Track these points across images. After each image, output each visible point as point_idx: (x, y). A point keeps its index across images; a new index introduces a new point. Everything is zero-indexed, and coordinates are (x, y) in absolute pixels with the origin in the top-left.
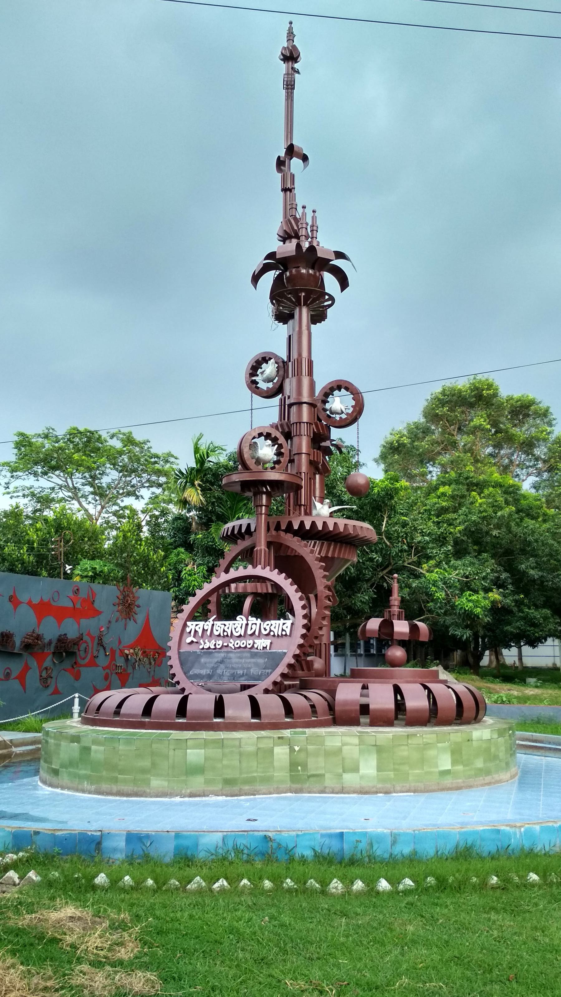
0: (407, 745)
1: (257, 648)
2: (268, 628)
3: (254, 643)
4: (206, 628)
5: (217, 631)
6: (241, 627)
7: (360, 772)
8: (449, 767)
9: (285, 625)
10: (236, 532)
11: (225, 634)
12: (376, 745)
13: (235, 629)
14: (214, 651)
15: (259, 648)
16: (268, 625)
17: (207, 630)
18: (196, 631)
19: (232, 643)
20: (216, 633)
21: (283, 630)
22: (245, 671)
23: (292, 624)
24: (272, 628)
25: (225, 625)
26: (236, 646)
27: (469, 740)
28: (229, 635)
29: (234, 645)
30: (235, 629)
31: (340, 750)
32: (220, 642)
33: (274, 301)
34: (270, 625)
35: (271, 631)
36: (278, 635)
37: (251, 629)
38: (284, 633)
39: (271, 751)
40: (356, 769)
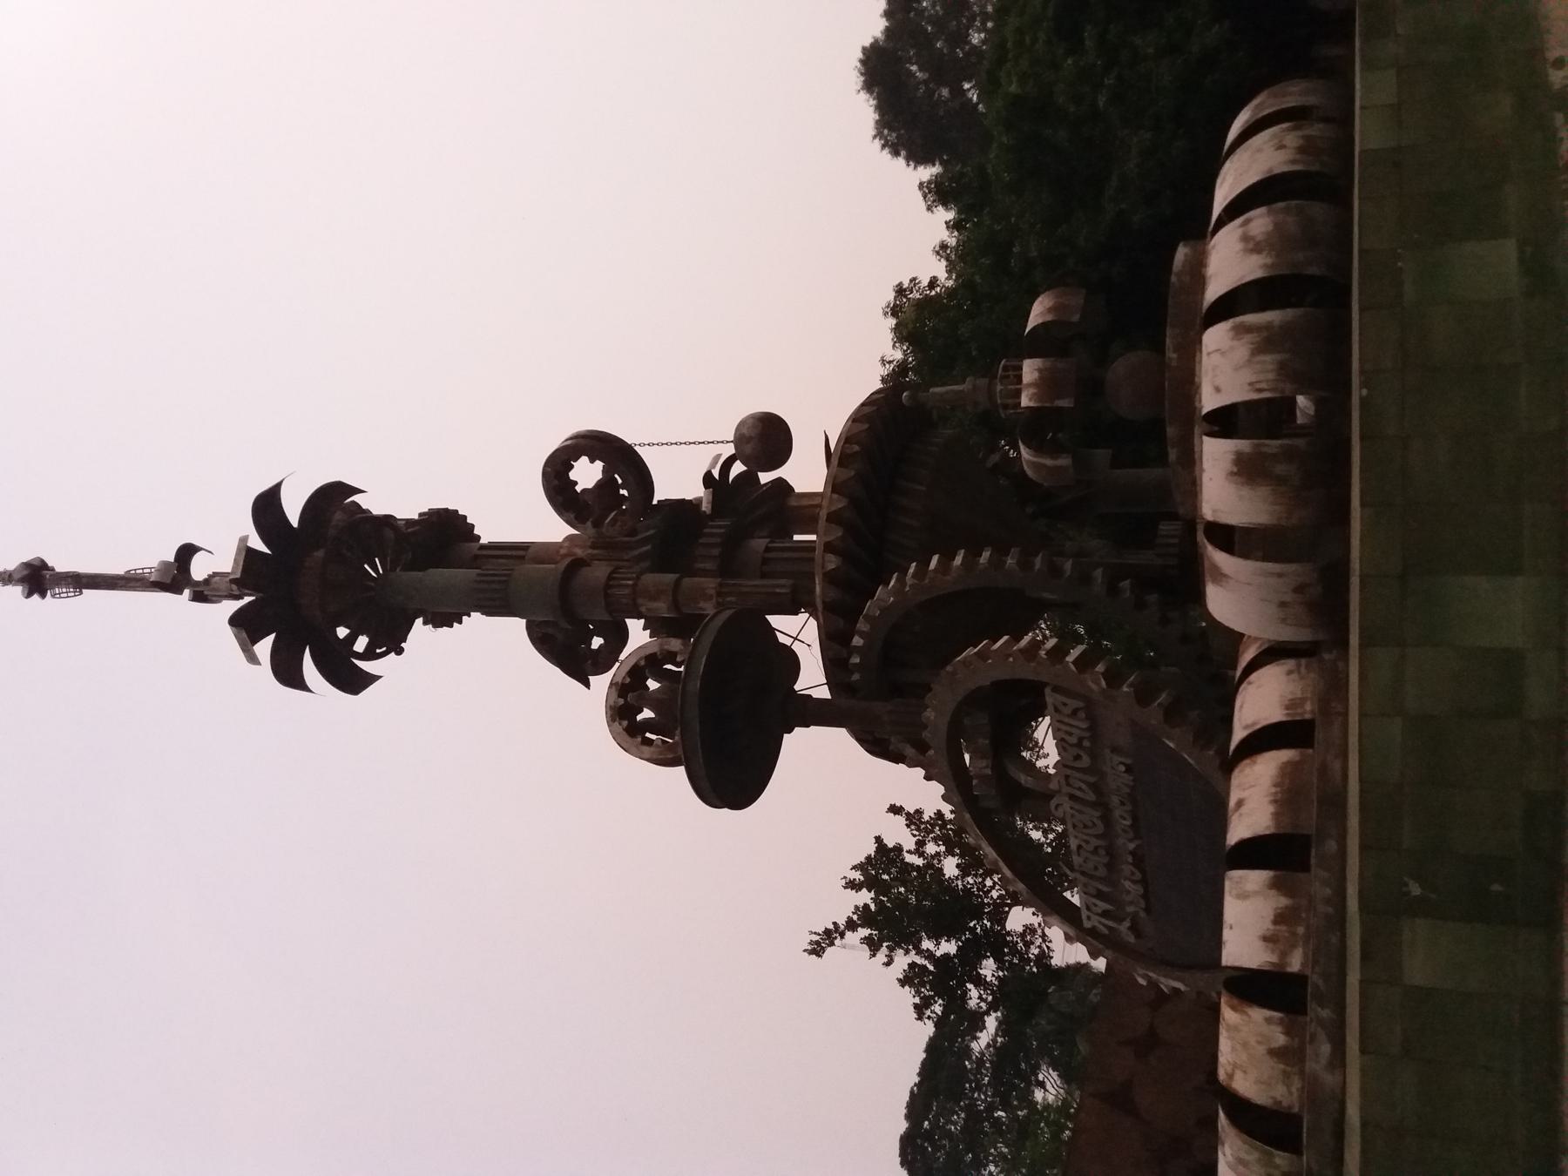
4: (1094, 892)
5: (1096, 868)
13: (1085, 826)
15: (1131, 784)
17: (1099, 891)
18: (1105, 914)
20: (1102, 872)
23: (1056, 689)
24: (1074, 740)
25: (1079, 847)
26: (1131, 835)
30: (1085, 826)
33: (378, 651)
35: (1079, 745)
36: (1088, 729)
37: (1080, 789)
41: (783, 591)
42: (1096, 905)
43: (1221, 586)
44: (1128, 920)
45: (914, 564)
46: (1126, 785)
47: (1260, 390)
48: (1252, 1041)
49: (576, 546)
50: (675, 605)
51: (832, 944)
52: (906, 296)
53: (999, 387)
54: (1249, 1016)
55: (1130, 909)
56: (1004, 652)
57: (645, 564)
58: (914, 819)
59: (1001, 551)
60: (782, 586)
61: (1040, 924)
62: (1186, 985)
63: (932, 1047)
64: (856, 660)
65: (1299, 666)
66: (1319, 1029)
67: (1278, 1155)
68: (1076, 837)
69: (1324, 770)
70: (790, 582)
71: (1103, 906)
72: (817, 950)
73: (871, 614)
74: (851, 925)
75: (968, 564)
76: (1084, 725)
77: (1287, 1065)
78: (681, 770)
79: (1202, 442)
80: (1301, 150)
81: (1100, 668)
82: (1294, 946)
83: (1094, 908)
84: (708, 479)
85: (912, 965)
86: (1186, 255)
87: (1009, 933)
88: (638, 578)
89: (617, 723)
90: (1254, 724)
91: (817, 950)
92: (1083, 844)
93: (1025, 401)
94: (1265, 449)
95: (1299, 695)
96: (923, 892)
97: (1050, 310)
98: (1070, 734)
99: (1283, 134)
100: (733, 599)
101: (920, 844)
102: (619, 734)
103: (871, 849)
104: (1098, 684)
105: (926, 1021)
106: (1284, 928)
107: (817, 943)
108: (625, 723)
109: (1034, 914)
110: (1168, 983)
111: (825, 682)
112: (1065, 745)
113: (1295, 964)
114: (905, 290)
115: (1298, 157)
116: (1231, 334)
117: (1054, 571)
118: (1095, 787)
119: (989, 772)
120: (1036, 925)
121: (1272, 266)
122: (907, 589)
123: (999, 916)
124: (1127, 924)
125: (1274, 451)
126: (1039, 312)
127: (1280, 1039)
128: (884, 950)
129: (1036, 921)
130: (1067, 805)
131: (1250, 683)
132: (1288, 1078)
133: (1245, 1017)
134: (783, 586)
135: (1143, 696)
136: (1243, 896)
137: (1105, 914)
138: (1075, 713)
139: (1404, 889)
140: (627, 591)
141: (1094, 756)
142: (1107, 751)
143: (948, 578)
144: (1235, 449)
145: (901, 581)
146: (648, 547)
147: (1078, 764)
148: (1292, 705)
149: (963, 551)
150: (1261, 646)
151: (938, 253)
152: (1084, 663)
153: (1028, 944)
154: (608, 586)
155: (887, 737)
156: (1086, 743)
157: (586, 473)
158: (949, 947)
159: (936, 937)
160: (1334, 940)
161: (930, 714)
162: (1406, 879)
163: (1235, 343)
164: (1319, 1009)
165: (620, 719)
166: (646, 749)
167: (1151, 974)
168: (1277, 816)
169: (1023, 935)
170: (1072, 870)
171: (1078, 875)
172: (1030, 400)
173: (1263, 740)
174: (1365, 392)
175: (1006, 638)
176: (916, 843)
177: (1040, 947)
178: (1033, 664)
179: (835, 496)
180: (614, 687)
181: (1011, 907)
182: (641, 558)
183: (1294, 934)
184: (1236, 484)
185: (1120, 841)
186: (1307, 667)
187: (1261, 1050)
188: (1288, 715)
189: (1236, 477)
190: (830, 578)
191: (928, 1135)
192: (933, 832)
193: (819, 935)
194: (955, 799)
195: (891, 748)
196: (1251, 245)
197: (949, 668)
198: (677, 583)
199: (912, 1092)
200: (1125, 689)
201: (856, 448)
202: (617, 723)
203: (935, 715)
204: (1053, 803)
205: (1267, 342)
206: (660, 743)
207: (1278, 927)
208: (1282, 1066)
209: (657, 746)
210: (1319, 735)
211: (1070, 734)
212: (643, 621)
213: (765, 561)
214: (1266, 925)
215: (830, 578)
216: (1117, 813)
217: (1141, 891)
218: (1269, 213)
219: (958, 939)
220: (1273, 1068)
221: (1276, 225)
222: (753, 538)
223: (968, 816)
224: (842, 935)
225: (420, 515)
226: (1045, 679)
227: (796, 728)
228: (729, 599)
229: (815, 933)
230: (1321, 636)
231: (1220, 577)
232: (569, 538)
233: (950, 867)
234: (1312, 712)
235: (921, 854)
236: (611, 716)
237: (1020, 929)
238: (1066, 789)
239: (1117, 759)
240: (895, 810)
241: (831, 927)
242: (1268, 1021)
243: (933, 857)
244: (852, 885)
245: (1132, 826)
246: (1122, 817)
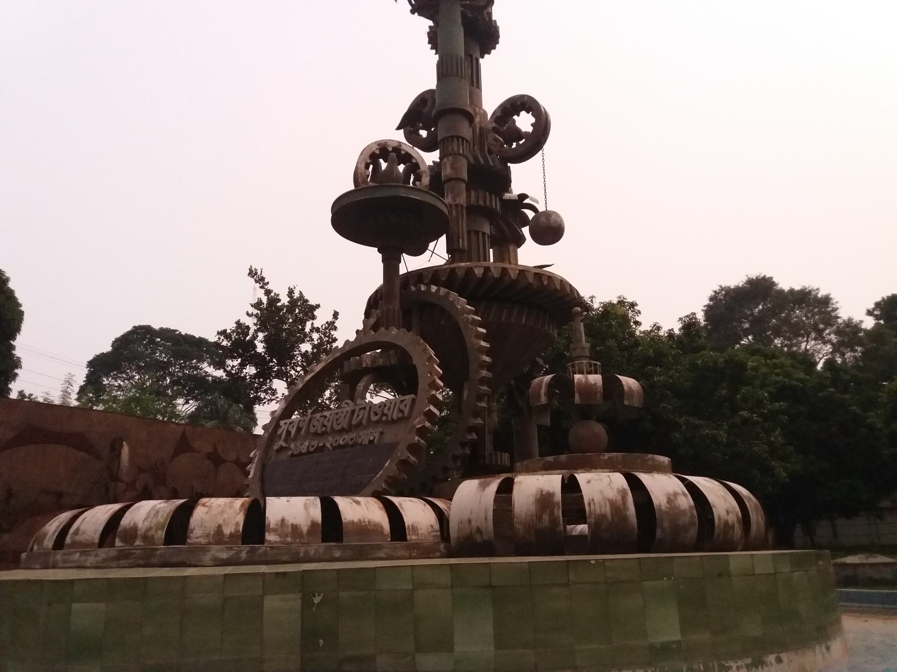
0: (567, 585)
1: (361, 444)
4: (300, 426)
5: (314, 426)
7: (458, 648)
8: (673, 635)
12: (490, 586)
15: (363, 444)
18: (289, 433)
19: (329, 442)
20: (312, 430)
23: (413, 400)
24: (386, 411)
25: (325, 417)
26: (334, 445)
27: (720, 575)
30: (337, 419)
32: (315, 443)
35: (383, 414)
36: (392, 419)
39: (259, 604)
40: (445, 644)
41: (461, 244)
42: (293, 427)
43: (478, 488)
44: (287, 445)
45: (480, 319)
46: (362, 441)
47: (589, 504)
48: (225, 516)
49: (481, 118)
50: (449, 180)
51: (256, 282)
52: (630, 308)
53: (584, 362)
54: (238, 514)
55: (292, 446)
56: (432, 372)
57: (472, 162)
58: (331, 326)
59: (490, 367)
60: (463, 243)
61: (277, 398)
62: (252, 478)
63: (201, 342)
64: (423, 288)
65: (436, 531)
66: (234, 552)
67: (163, 532)
68: (331, 415)
69: (380, 547)
70: (466, 249)
71: (293, 431)
72: (252, 273)
73: (450, 295)
74: (267, 293)
75: (481, 350)
76: (394, 417)
77: (213, 535)
78: (352, 187)
79: (559, 474)
80: (726, 523)
81: (427, 424)
82: (280, 536)
83: (291, 426)
84: (523, 196)
85: (248, 328)
86: (664, 462)
87: (271, 381)
88: (464, 156)
89: (377, 147)
90: (402, 508)
91: (252, 273)
92: (327, 419)
93: (577, 377)
94: (556, 508)
95: (419, 532)
96: (290, 333)
97: (630, 388)
98: (389, 409)
99: (735, 512)
100: (454, 214)
101: (318, 330)
102: (371, 148)
103: (312, 302)
104: (418, 424)
105: (217, 337)
106: (290, 530)
107: (256, 273)
108: (377, 152)
109: (283, 394)
110: (252, 469)
111: (409, 271)
112: (383, 407)
113: (270, 537)
114: (633, 308)
115: (722, 522)
116: (621, 488)
117: (480, 397)
118: (360, 424)
119: (364, 365)
120: (277, 396)
121: (660, 510)
122: (466, 316)
123: (280, 375)
124: (284, 445)
125: (556, 513)
126: (629, 382)
127: (227, 531)
128: (256, 312)
129: (279, 395)
130: (349, 409)
131: (425, 505)
132: (206, 536)
133: (238, 510)
134: (463, 244)
135: (413, 448)
136: (306, 507)
137: (289, 433)
138: (402, 411)
139: (316, 594)
140: (456, 149)
141: (377, 422)
142: (381, 430)
143: (473, 339)
144: (555, 492)
145: (470, 312)
146: (482, 162)
147: (372, 414)
148: (414, 529)
149: (489, 346)
150: (446, 510)
151: (655, 325)
152: (429, 415)
153: (266, 391)
154: (458, 137)
155: (379, 307)
156: (384, 418)
157: (524, 122)
158: (260, 348)
159: (266, 340)
160: (285, 558)
161: (394, 331)
162: (322, 595)
163: (615, 491)
164: (246, 551)
165: (380, 149)
166: (363, 166)
167: (256, 460)
168: (353, 522)
169: (271, 389)
170: (312, 413)
171: (309, 417)
172: (578, 379)
173: (394, 514)
174: (593, 562)
175: (441, 372)
176: (318, 327)
177: (265, 398)
178: (427, 387)
179: (517, 272)
180: (398, 144)
181: (286, 381)
182: (476, 158)
183: (287, 536)
184: (536, 494)
185: (330, 439)
186: (435, 535)
187: (221, 521)
188: (409, 526)
189: (539, 493)
190: (469, 271)
191: (152, 341)
192: (325, 336)
193: (261, 274)
194: (347, 347)
195: (373, 310)
196: (672, 498)
197: (422, 341)
198: (463, 180)
199: (176, 331)
200: (417, 438)
201: (546, 283)
202: (377, 147)
203: (394, 334)
204: (349, 401)
205: (617, 509)
206: (367, 173)
207: (290, 527)
208: (212, 533)
209: (365, 172)
210: (398, 544)
211: (389, 409)
212: (438, 160)
213: (477, 232)
214: (291, 520)
215: (469, 271)
216: (346, 437)
217: (303, 452)
218: (690, 507)
219: (265, 353)
220: (211, 528)
221: (684, 511)
222: (490, 225)
223: (338, 355)
224: (262, 287)
225: (495, 21)
226: (420, 393)
227: (381, 255)
228: (454, 211)
229: (262, 272)
230: (453, 542)
231: (483, 486)
232: (485, 113)
233: (306, 347)
234: (411, 540)
235: (311, 331)
236: (381, 143)
237: (274, 387)
238: (357, 408)
239: (377, 435)
240: (336, 315)
241: (266, 281)
242: (237, 524)
243: (311, 337)
244: (291, 292)
246: (344, 439)
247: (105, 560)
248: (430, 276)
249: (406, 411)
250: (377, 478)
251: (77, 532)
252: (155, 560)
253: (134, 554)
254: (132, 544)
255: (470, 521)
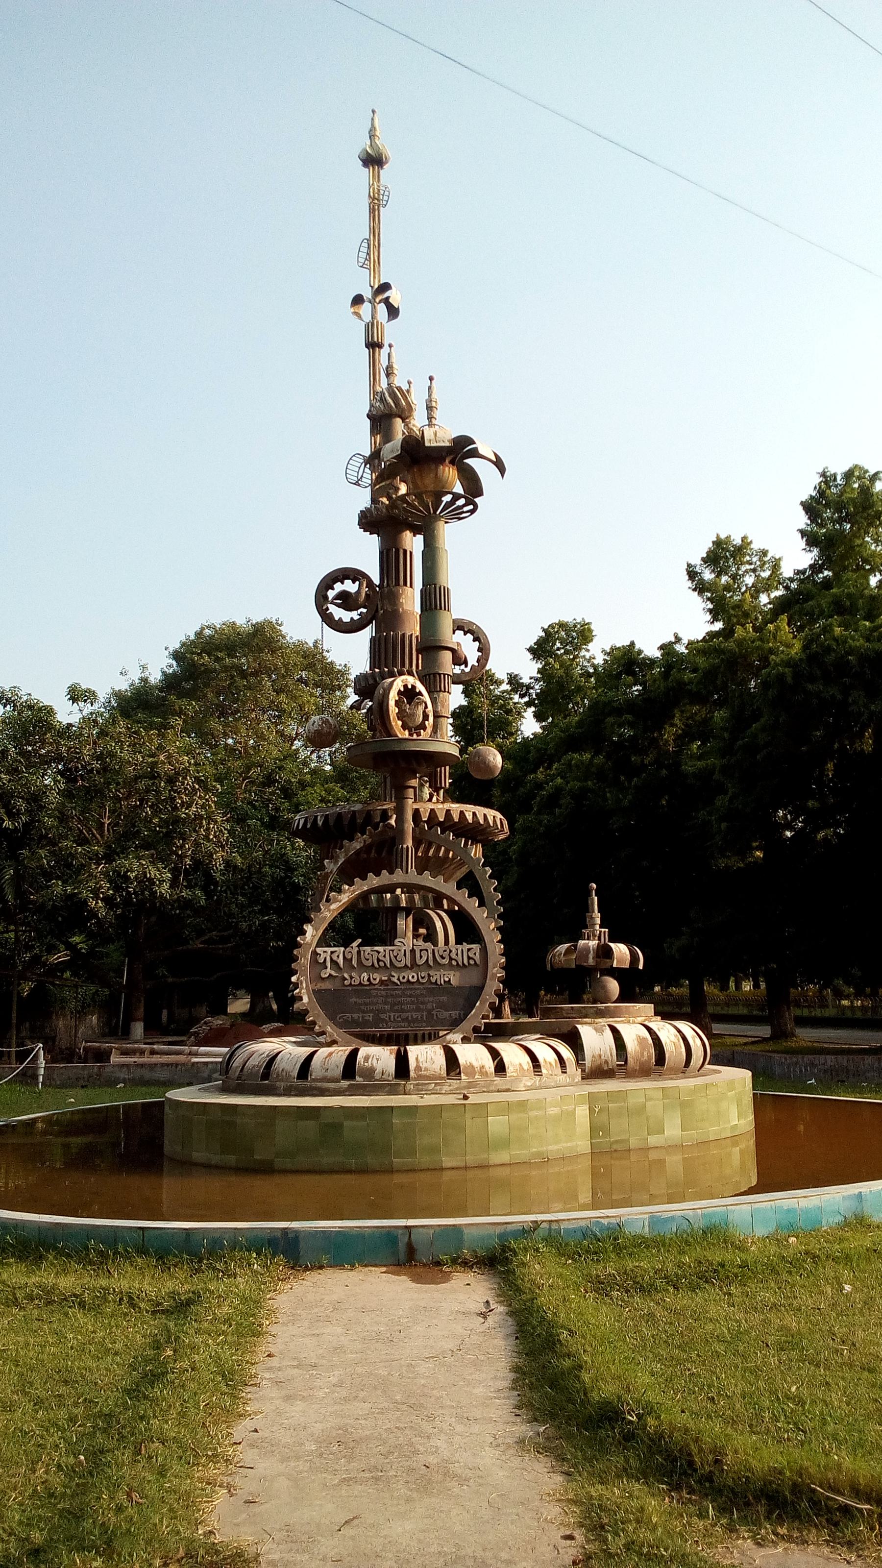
2: (446, 954)
3: (429, 976)
4: (349, 957)
5: (368, 960)
6: (405, 955)
9: (472, 952)
10: (320, 823)
11: (382, 964)
13: (396, 957)
14: (368, 988)
16: (445, 951)
17: (352, 959)
21: (469, 958)
22: (425, 1014)
24: (453, 956)
25: (378, 952)
28: (388, 965)
29: (398, 979)
30: (396, 957)
31: (645, 1106)
34: (448, 950)
35: (451, 959)
37: (421, 957)
38: (472, 962)
71: (341, 961)
245: (408, 981)
247: (457, 1089)
248: (428, 815)
249: (477, 958)
250: (472, 1016)
251: (419, 1068)
252: (492, 1088)
253: (479, 1084)
254: (474, 1078)
255: (600, 1056)
